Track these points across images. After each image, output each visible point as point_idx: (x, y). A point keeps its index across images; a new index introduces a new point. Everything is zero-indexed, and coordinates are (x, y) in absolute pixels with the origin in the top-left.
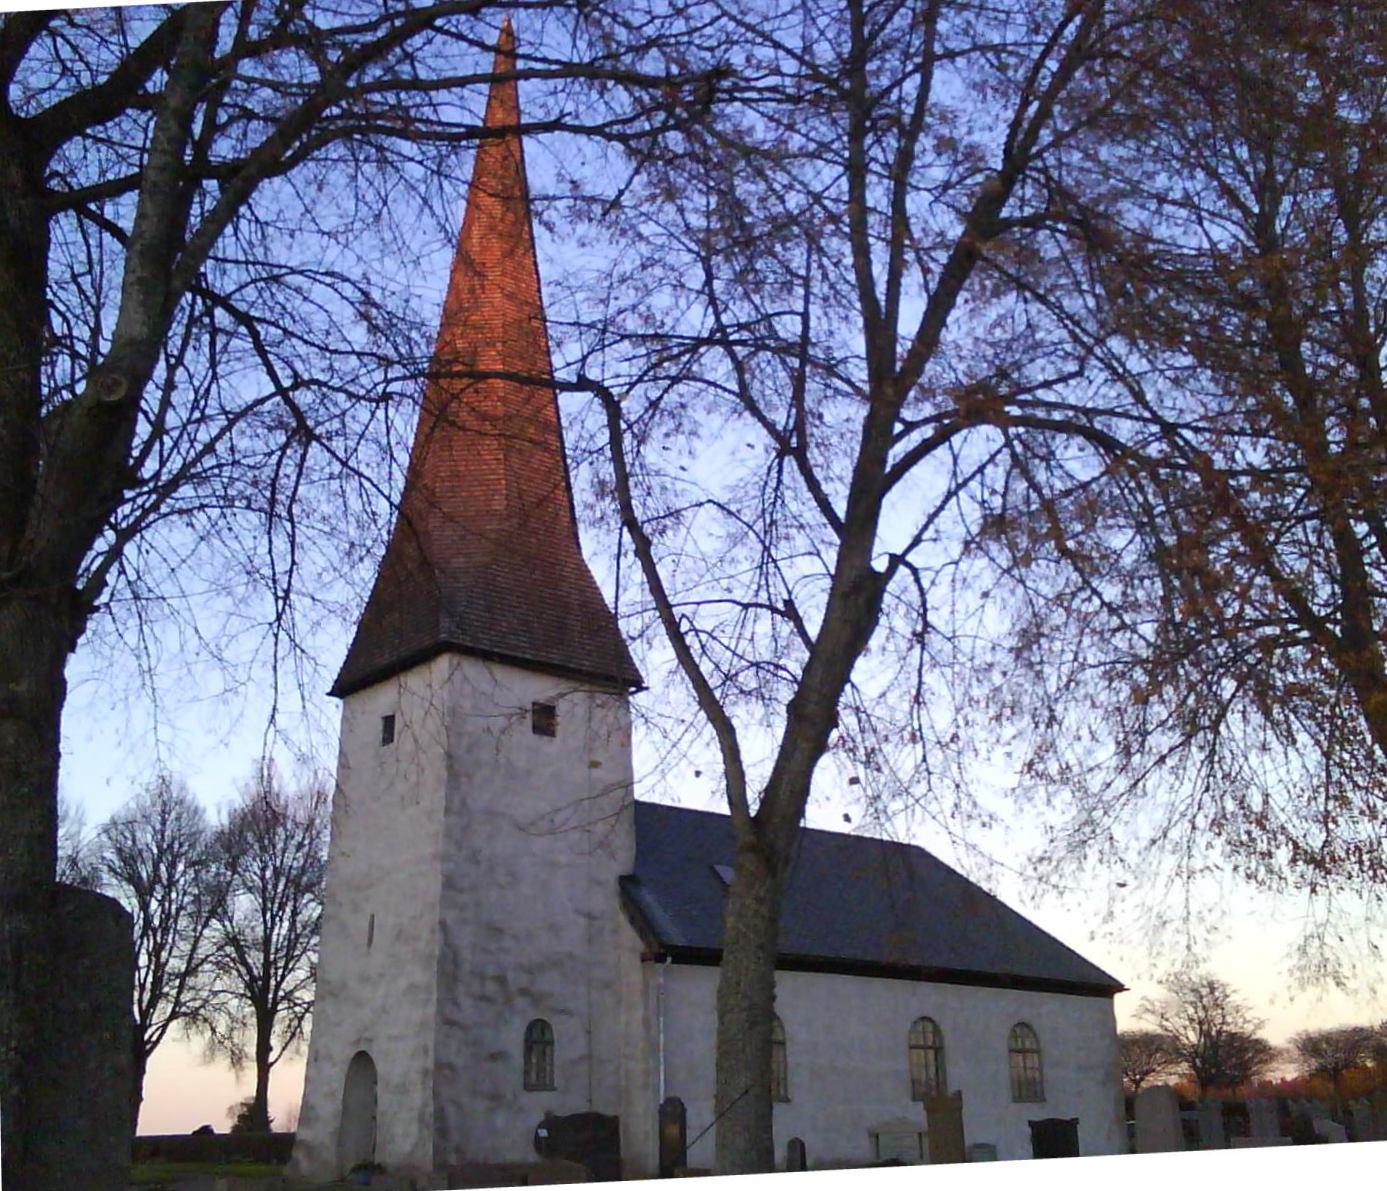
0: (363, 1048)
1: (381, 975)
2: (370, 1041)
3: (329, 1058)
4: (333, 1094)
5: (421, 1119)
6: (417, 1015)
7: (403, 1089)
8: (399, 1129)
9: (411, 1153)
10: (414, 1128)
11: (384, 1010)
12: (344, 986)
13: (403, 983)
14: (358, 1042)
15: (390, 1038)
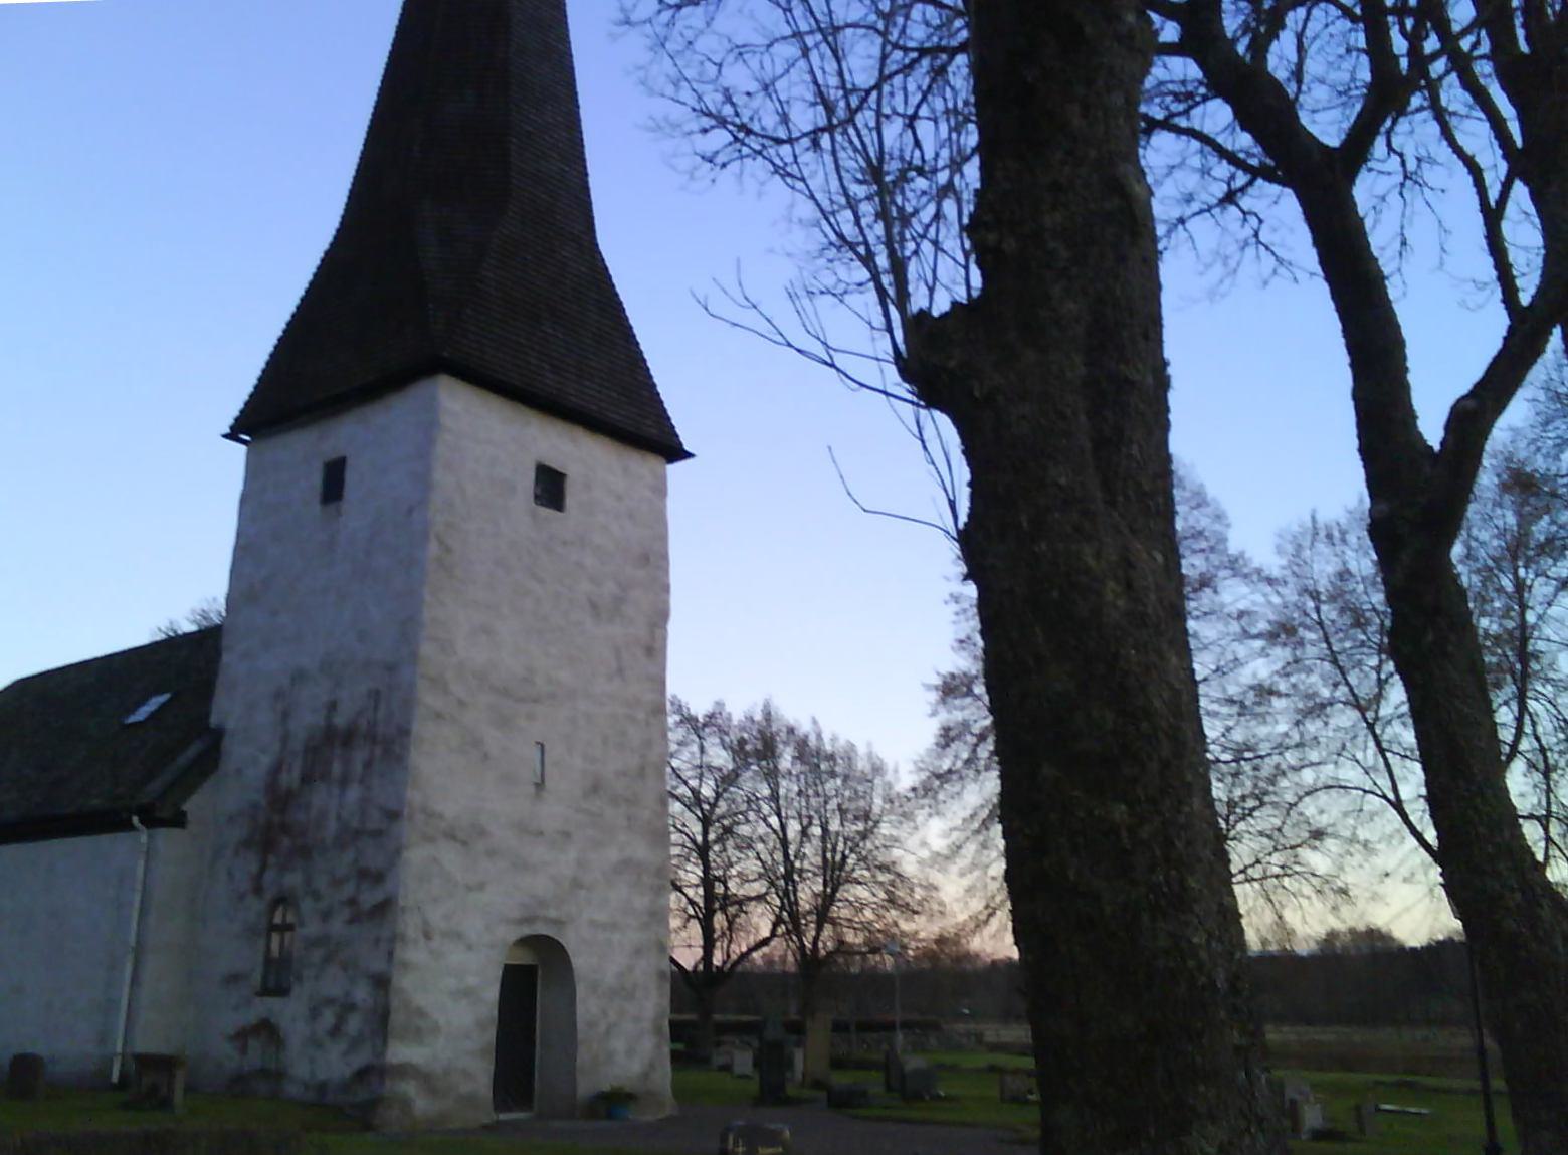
0: (541, 929)
1: (567, 835)
2: (558, 923)
3: (457, 936)
4: (467, 993)
5: (658, 1031)
6: (641, 902)
7: (624, 992)
8: (619, 1045)
9: (646, 1075)
10: (648, 1045)
11: (576, 884)
12: (483, 833)
13: (613, 855)
14: (528, 920)
15: (593, 923)
